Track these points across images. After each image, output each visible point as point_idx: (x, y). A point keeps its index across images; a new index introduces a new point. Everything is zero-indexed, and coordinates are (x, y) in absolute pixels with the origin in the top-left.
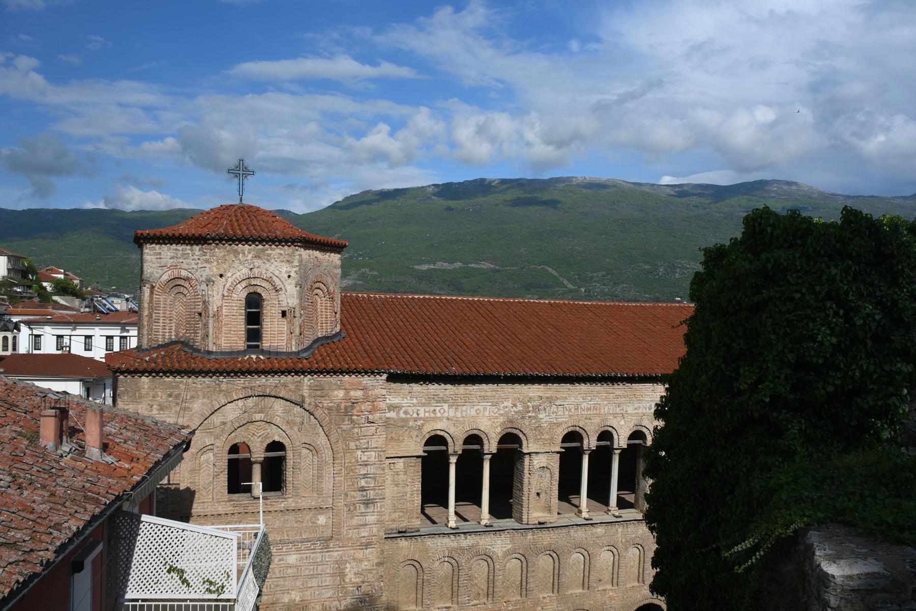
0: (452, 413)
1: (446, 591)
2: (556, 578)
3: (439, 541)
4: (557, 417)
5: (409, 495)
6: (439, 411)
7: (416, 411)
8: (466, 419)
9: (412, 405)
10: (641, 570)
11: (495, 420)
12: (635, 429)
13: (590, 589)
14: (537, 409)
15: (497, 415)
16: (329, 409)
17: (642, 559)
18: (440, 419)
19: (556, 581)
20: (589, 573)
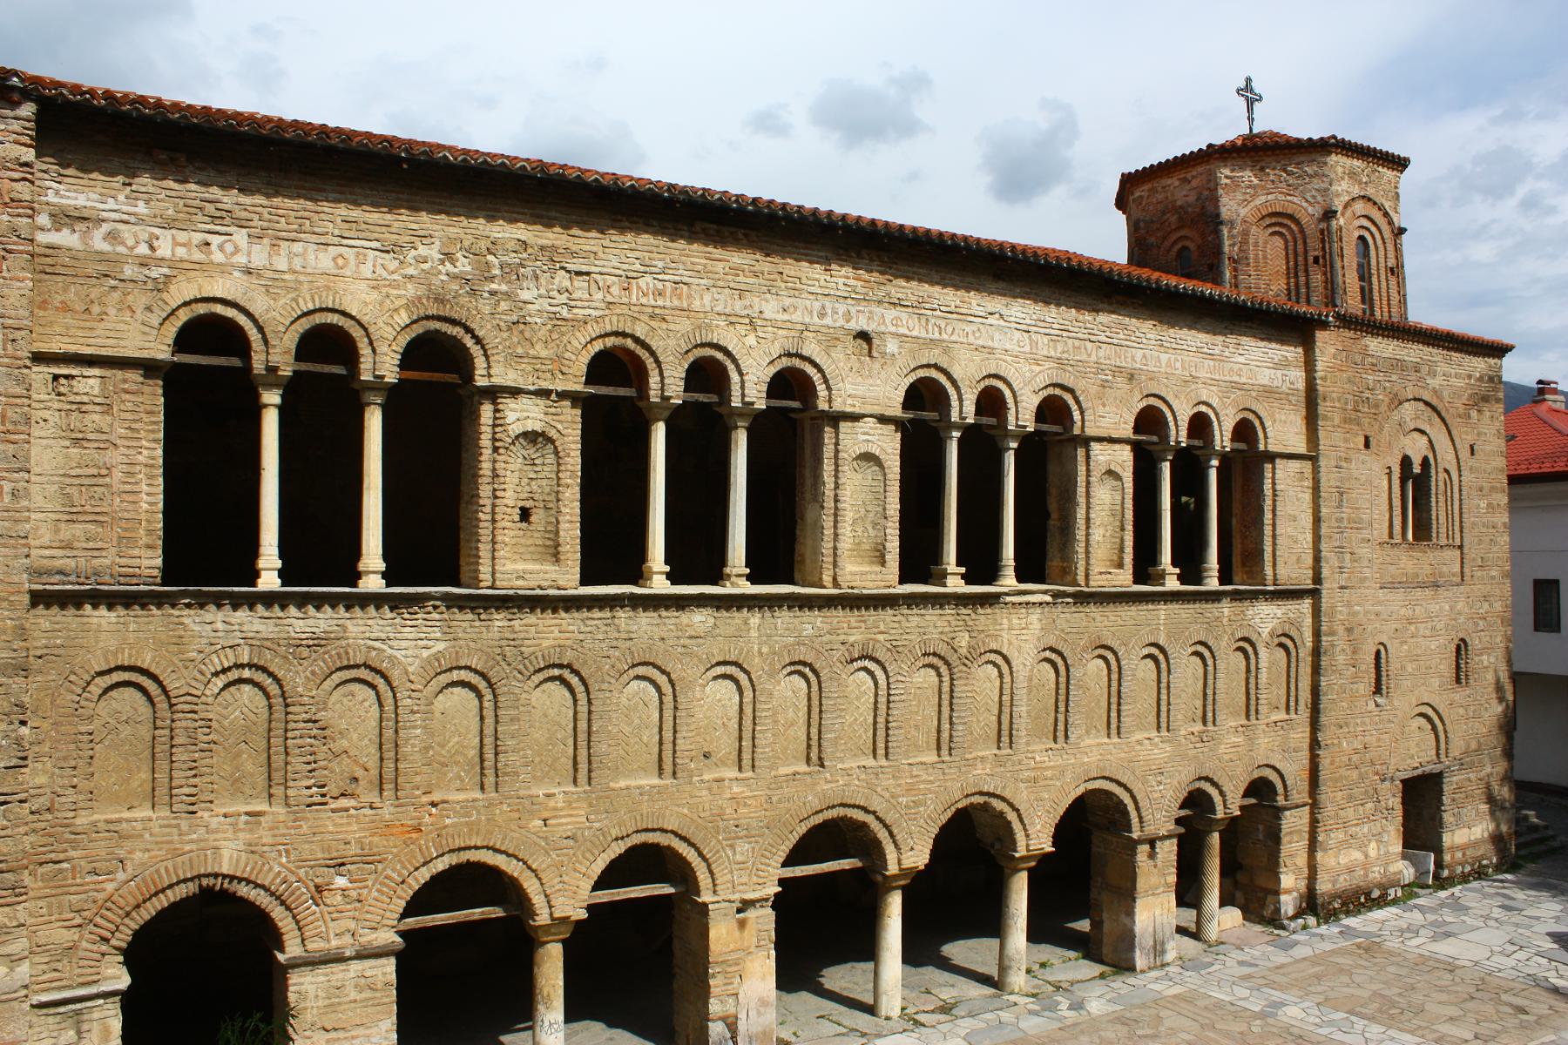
0: (259, 255)
1: (249, 767)
2: (582, 743)
3: (220, 616)
4: (573, 303)
5: (117, 475)
6: (221, 248)
7: (146, 236)
8: (302, 278)
9: (133, 219)
10: (814, 730)
11: (395, 292)
12: (786, 362)
13: (678, 775)
14: (512, 273)
15: (395, 277)
17: (815, 702)
18: (224, 269)
19: (583, 753)
20: (675, 732)
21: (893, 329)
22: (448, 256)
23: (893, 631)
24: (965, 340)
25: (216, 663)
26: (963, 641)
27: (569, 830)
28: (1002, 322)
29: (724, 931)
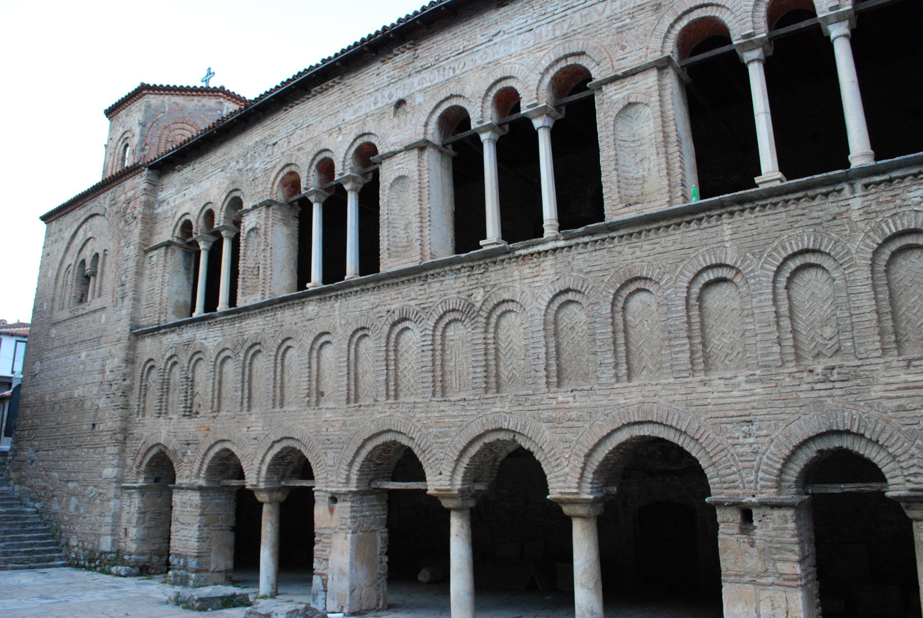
12: (359, 142)
16: (117, 213)
21: (419, 88)
22: (237, 162)
23: (421, 297)
24: (474, 66)
25: (168, 355)
26: (479, 296)
27: (253, 435)
28: (506, 36)
29: (321, 512)
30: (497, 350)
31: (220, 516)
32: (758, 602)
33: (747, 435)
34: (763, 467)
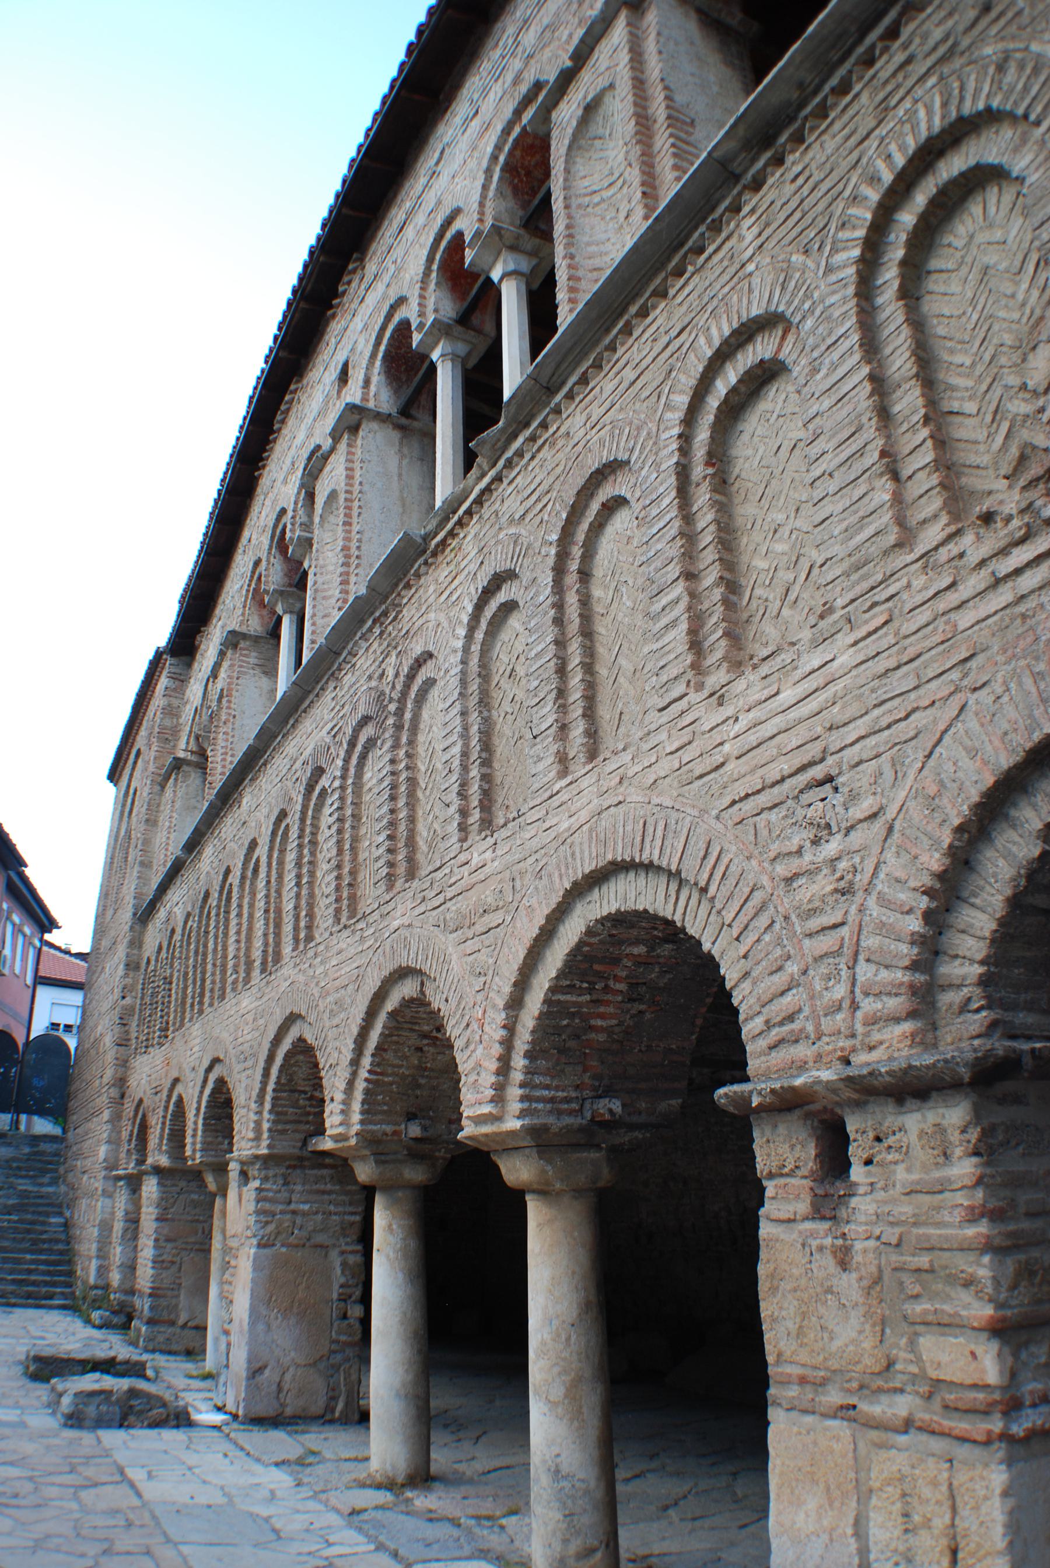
30: (412, 782)
31: (200, 1226)
32: (864, 1494)
33: (822, 831)
34: (870, 942)
